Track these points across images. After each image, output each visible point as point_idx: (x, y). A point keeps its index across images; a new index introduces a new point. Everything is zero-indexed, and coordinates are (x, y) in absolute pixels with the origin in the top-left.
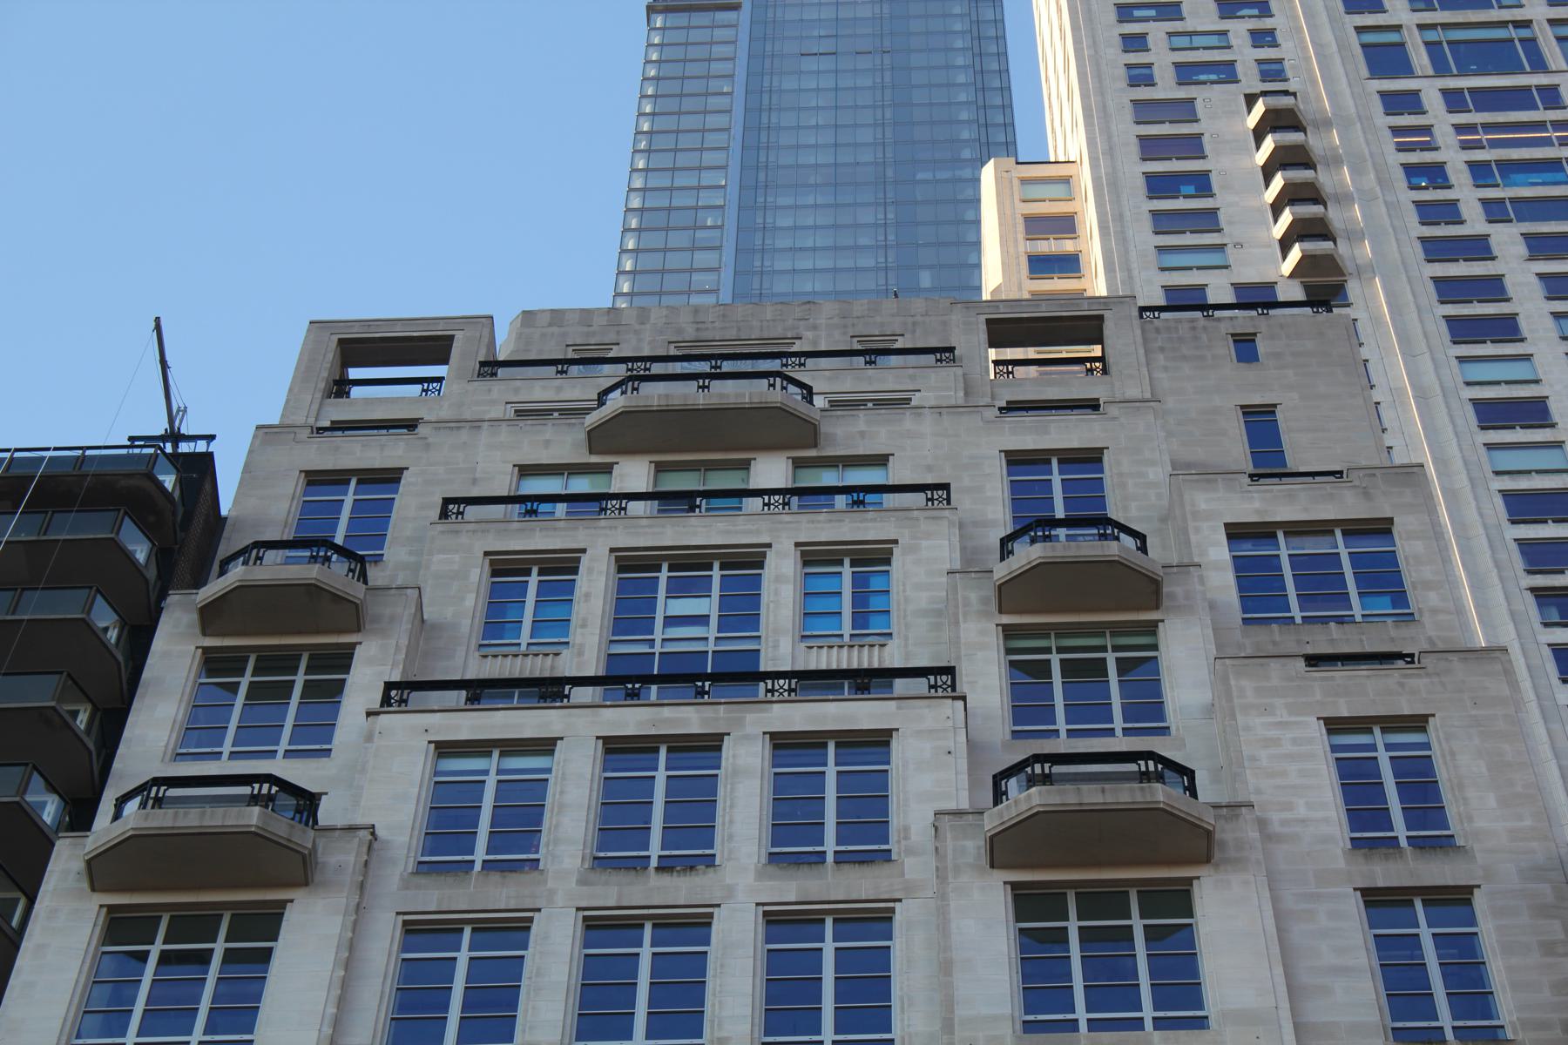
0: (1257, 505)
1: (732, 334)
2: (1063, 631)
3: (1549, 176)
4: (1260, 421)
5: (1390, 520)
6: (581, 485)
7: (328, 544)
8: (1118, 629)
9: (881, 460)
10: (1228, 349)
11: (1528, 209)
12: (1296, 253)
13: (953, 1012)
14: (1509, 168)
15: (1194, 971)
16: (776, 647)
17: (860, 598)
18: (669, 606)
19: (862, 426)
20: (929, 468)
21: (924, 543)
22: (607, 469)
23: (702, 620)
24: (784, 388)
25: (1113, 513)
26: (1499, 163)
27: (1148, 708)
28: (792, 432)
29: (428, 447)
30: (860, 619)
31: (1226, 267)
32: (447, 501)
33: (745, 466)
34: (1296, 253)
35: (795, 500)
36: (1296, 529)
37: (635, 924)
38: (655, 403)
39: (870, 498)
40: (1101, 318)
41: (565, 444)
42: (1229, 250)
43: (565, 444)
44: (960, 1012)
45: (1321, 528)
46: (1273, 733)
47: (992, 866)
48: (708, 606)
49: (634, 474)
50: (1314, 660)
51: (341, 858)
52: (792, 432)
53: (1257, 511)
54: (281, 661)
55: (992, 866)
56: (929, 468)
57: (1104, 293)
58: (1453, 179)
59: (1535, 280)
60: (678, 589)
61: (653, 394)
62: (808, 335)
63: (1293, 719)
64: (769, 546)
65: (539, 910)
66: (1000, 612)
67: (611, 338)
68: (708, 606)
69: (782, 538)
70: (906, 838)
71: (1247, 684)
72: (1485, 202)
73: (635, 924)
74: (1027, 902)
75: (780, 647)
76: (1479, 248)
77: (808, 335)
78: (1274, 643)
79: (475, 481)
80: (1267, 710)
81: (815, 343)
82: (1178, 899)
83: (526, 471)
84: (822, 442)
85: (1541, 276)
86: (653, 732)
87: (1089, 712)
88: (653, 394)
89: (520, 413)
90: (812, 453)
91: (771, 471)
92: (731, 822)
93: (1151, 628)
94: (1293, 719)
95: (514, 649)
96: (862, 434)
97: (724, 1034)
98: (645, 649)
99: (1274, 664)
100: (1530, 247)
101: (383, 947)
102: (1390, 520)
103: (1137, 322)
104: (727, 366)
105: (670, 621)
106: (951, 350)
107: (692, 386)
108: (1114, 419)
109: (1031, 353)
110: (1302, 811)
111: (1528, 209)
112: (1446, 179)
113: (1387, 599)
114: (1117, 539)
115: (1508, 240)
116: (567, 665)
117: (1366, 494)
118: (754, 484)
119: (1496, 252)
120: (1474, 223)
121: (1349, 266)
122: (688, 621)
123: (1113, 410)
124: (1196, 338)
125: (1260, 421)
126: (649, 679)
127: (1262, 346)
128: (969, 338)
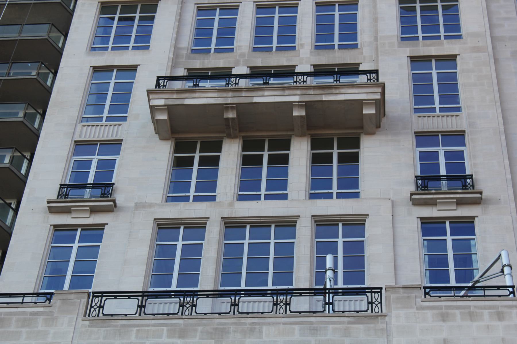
13: (377, 34)
15: (458, 20)
37: (273, 7)
44: (380, 34)
65: (241, 2)
73: (273, 7)
97: (302, 42)
101: (191, 16)
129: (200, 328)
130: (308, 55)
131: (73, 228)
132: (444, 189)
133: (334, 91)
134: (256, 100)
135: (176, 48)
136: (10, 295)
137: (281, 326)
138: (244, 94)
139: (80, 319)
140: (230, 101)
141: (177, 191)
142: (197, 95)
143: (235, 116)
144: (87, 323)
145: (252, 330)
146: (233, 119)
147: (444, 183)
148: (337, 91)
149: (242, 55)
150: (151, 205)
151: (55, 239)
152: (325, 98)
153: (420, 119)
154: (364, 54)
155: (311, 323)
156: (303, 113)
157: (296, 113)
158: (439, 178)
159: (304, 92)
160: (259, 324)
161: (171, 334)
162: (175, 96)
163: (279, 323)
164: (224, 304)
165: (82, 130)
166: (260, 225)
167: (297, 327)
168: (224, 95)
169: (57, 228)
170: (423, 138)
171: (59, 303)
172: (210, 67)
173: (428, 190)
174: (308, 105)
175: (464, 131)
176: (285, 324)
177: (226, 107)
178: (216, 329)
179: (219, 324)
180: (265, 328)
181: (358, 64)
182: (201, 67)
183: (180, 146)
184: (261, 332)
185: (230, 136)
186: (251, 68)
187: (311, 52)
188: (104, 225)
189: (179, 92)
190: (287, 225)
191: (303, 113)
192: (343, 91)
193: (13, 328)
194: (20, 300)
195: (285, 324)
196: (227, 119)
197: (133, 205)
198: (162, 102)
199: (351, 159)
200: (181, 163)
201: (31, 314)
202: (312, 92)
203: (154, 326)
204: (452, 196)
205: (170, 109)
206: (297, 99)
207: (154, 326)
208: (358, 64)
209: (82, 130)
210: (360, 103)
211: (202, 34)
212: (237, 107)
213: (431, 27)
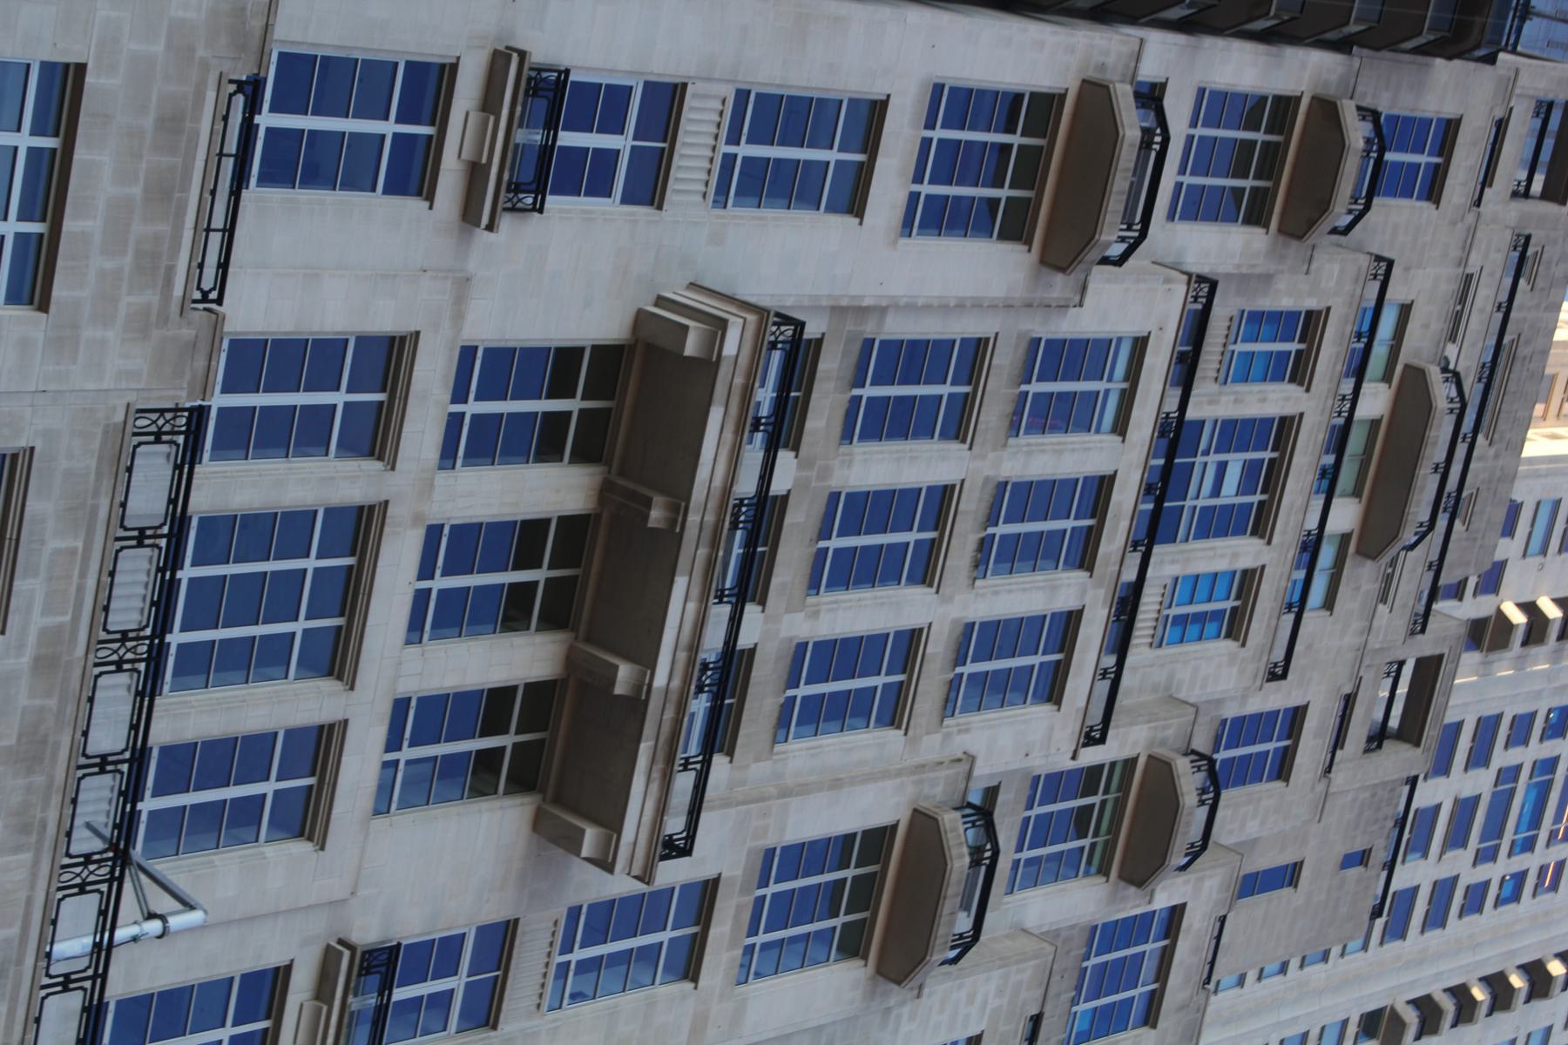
0: (1196, 925)
1: (1512, 387)
2: (1120, 805)
3: (1526, 819)
4: (1289, 875)
5: (1154, 1026)
6: (1380, 352)
7: (1382, 151)
8: (1110, 847)
9: (1329, 604)
10: (1358, 846)
11: (1501, 803)
12: (1518, 618)
13: (797, 795)
14: (1544, 790)
16: (1173, 562)
17: (1201, 618)
18: (1235, 462)
19: (1364, 588)
20: (1309, 647)
21: (1235, 670)
22: (1387, 378)
23: (1216, 491)
24: (1452, 411)
25: (1226, 795)
26: (1550, 783)
27: (1033, 874)
28: (1376, 537)
29: (1453, 223)
30: (1182, 621)
31: (1524, 556)
32: (1390, 264)
33: (1357, 493)
34: (1518, 618)
35: (1341, 421)
36: (1166, 957)
38: (1418, 483)
39: (1325, 483)
40: (1417, 744)
41: (1419, 343)
42: (1540, 559)
43: (1419, 343)
44: (794, 802)
45: (1162, 973)
46: (979, 1000)
47: (915, 810)
48: (1230, 493)
49: (1375, 401)
50: (1036, 1020)
51: (1060, 286)
52: (1376, 537)
53: (1190, 926)
54: (1271, 158)
55: (915, 810)
56: (1309, 647)
57: (1529, 451)
58: (1548, 744)
59: (1436, 802)
60: (1251, 469)
61: (1441, 430)
62: (1492, 451)
63: (988, 1012)
64: (1269, 543)
66: (1150, 756)
67: (1540, 283)
68: (1230, 493)
69: (1272, 557)
70: (960, 732)
71: (1027, 975)
72: (1518, 769)
74: (877, 840)
75: (1169, 563)
76: (1480, 758)
77: (1492, 451)
78: (1058, 995)
79: (1407, 269)
80: (1000, 992)
81: (1481, 458)
82: (852, 945)
83: (1405, 311)
84: (1359, 558)
85: (1438, 807)
86: (1109, 515)
87: (1042, 831)
88: (1441, 430)
89: (1469, 278)
90: (1352, 549)
91: (1345, 515)
92: (1010, 591)
93: (1104, 871)
94: (988, 1012)
95: (1232, 338)
96: (1358, 589)
97: (822, 615)
98: (1203, 446)
99: (1040, 992)
100: (1466, 800)
102: (1154, 1026)
103: (1405, 775)
104: (1461, 449)
105: (1222, 467)
106: (1423, 631)
107: (1440, 455)
108: (1313, 788)
109: (1402, 690)
110: (905, 1027)
111: (1501, 803)
112: (1551, 737)
113: (1086, 1026)
114: (1202, 803)
115: (1481, 783)
116: (1203, 387)
117: (1183, 1007)
118: (1367, 387)
119: (1472, 773)
120: (1502, 757)
121: (1494, 656)
122: (1219, 478)
123: (1321, 787)
124: (1376, 821)
125: (1289, 875)
126: (1159, 502)
127: (1354, 872)
128: (1426, 646)
129: (52, 703)
130: (785, 632)
131: (440, 118)
132: (354, 1003)
133: (659, 766)
134: (680, 583)
135: (882, 311)
136: (224, 266)
137: (23, 895)
138: (703, 552)
139: (131, 397)
140: (693, 518)
141: (489, 368)
142: (729, 436)
143: (650, 525)
144: (119, 417)
145: (25, 829)
146: (646, 517)
147: (372, 1001)
148: (656, 775)
149: (825, 473)
150: (458, 317)
151: (416, 70)
152: (645, 748)
153: (551, 924)
154: (754, 766)
155: (20, 962)
156: (619, 690)
157: (625, 673)
158: (386, 987)
159: (673, 697)
160: (40, 841)
161: (53, 638)
162: (739, 381)
163: (32, 888)
164: (109, 736)
165: (710, 110)
166: (349, 594)
167: (15, 930)
168: (712, 504)
169: (447, 73)
170: (500, 941)
171: (187, 333)
172: (814, 396)
173: (360, 975)
174: (637, 704)
175: (494, 1027)
176: (29, 902)
177: (679, 508)
178: (44, 741)
179: (57, 745)
180: (27, 857)
181: (730, 753)
182: (818, 375)
183: (608, 357)
184: (17, 849)
185: (606, 490)
186: (819, 342)
187: (791, 639)
188: (430, 198)
189: (748, 391)
190: (336, 658)
191: (619, 690)
192: (655, 787)
193: (139, 228)
194: (218, 221)
195: (29, 902)
196: (648, 504)
197: (472, 266)
198: (730, 348)
199: (481, 777)
200: (561, 368)
201: (171, 270)
202: (669, 714)
203: (81, 589)
204: (332, 1031)
205: (708, 366)
206: (660, 680)
207: (81, 589)
208: (730, 753)
209: (715, 97)
210: (648, 661)
211: (911, 359)
212: (672, 537)
213: (785, 910)
